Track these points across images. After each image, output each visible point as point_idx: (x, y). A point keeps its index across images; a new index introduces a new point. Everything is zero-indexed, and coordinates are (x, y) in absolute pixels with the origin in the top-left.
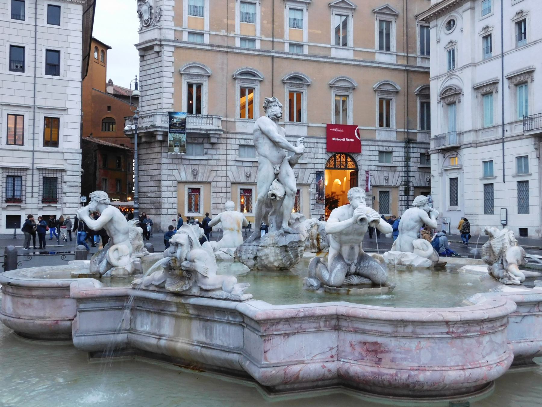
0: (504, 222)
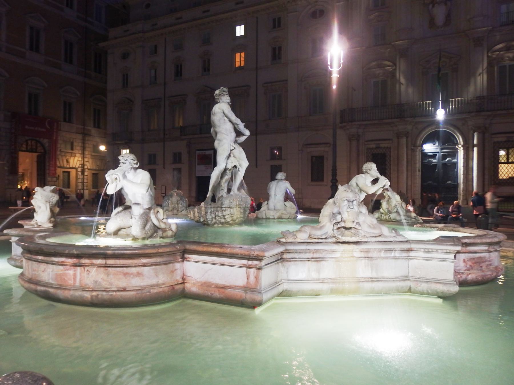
0: (164, 195)
